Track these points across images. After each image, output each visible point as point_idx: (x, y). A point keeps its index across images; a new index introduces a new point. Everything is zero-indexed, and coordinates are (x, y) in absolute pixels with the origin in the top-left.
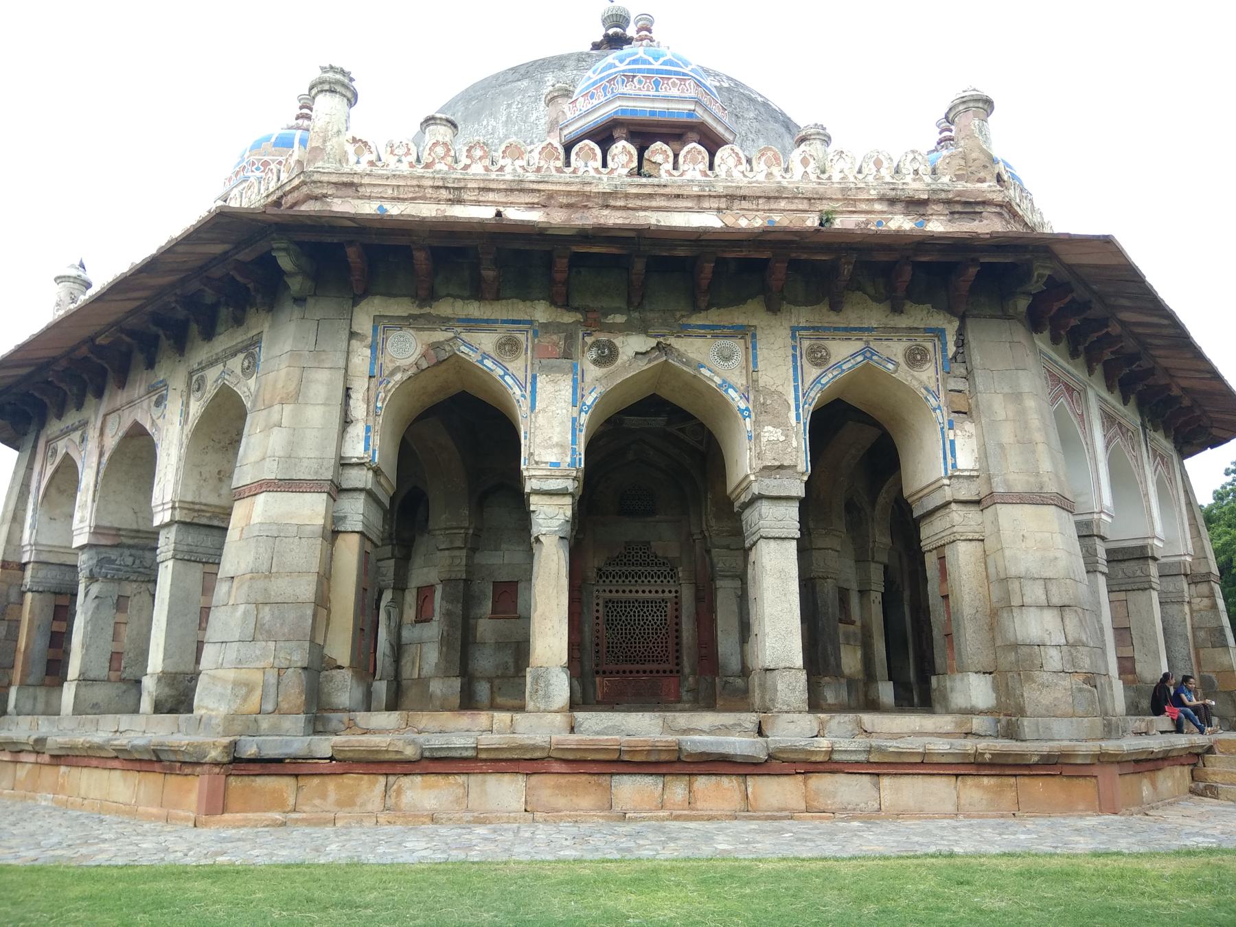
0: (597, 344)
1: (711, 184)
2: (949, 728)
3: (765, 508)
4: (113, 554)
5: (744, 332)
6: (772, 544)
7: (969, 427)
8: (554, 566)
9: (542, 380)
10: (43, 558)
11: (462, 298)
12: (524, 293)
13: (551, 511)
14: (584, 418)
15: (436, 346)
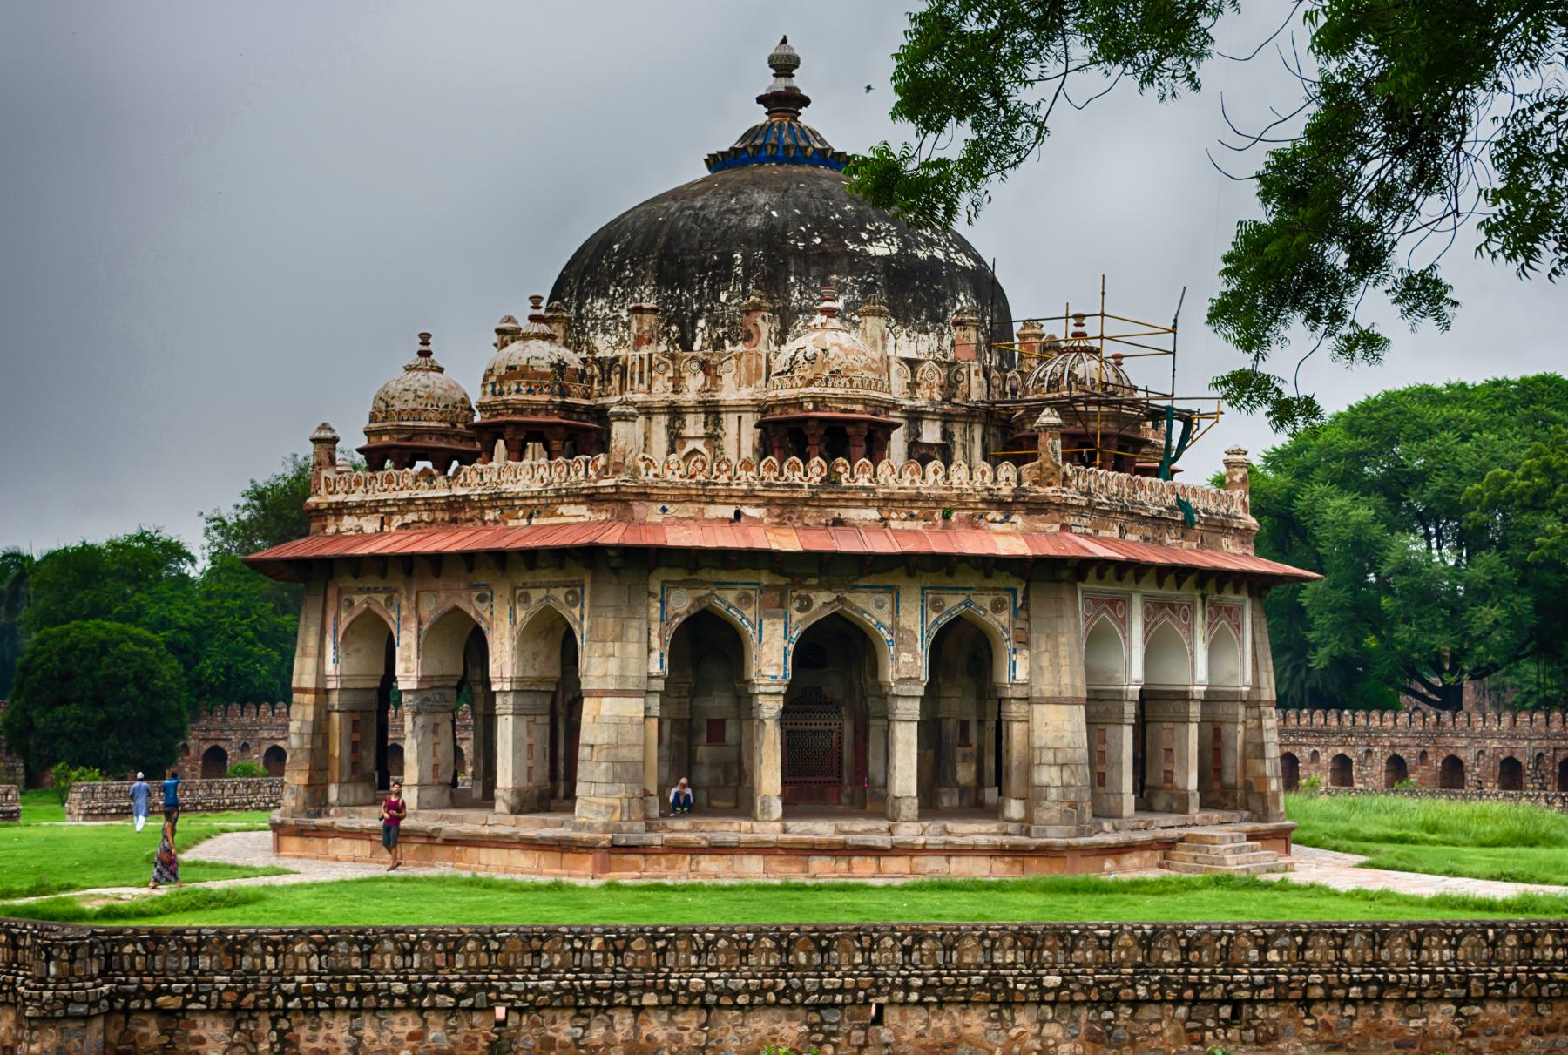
0: (799, 597)
1: (873, 490)
2: (994, 830)
3: (900, 703)
4: (429, 694)
5: (893, 591)
6: (903, 724)
7: (1025, 653)
8: (772, 738)
9: (765, 622)
10: (346, 685)
11: (716, 568)
12: (756, 568)
13: (771, 704)
14: (791, 647)
15: (699, 599)
